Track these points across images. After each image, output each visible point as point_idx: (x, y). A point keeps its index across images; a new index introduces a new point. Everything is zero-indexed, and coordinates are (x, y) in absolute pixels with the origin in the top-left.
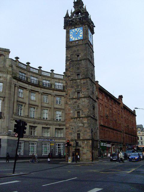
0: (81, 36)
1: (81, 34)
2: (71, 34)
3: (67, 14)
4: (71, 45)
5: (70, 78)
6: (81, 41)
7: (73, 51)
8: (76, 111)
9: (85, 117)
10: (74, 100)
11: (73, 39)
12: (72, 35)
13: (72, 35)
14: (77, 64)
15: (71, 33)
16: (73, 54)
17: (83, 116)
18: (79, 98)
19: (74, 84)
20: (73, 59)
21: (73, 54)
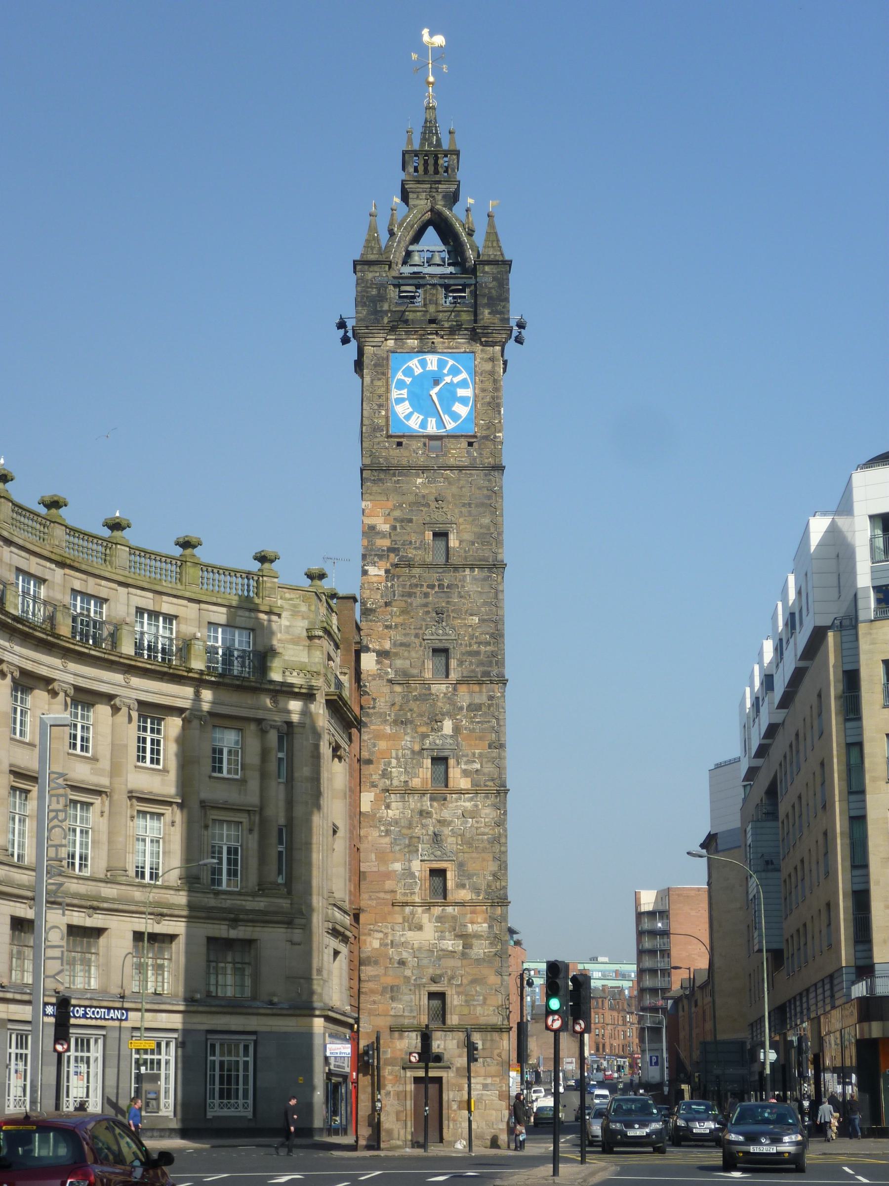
0: (462, 410)
1: (464, 401)
2: (401, 385)
3: (371, 240)
4: (397, 456)
5: (387, 662)
6: (464, 444)
7: (412, 498)
9: (473, 904)
10: (413, 802)
11: (414, 423)
12: (404, 393)
13: (404, 393)
14: (432, 587)
15: (400, 375)
16: (410, 521)
17: (464, 895)
19: (413, 705)
20: (411, 553)
21: (410, 521)
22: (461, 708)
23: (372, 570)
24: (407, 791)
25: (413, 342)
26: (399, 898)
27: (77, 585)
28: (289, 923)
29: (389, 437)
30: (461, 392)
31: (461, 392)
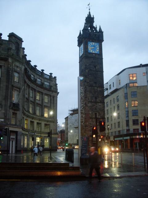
0: (98, 51)
1: (98, 49)
6: (98, 55)
8: (94, 113)
11: (91, 51)
15: (89, 45)
17: (99, 117)
18: (96, 102)
22: (98, 91)
23: (86, 71)
24: (91, 102)
25: (91, 41)
26: (91, 117)
27: (32, 73)
28: (53, 122)
29: (88, 53)
30: (97, 48)
31: (97, 48)
